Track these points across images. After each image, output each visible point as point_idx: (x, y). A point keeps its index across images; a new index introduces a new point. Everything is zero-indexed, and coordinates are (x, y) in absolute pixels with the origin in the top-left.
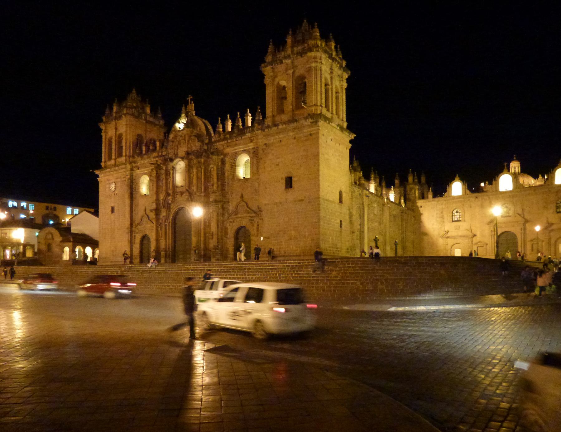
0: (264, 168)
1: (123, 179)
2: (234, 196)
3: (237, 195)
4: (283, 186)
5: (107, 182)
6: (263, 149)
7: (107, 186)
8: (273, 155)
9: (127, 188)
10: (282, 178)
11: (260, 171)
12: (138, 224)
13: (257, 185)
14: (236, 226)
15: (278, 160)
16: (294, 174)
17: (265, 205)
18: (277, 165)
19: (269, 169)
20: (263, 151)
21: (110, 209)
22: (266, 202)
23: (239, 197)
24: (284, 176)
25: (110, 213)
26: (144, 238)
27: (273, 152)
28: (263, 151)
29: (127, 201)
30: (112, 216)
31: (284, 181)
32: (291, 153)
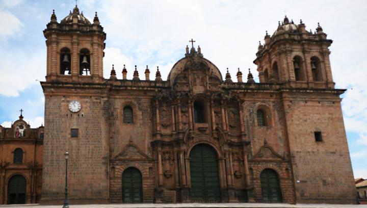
0: (292, 120)
1: (95, 101)
2: (255, 139)
3: (259, 140)
4: (312, 138)
5: (63, 99)
6: (288, 105)
7: (62, 103)
8: (299, 111)
9: (102, 112)
10: (311, 132)
11: (288, 123)
12: (120, 155)
13: (280, 134)
14: (262, 167)
15: (305, 117)
16: (322, 131)
17: (297, 152)
18: (305, 121)
19: (297, 122)
20: (290, 107)
21: (69, 132)
22: (298, 150)
23: (262, 142)
24: (314, 130)
25: (70, 136)
26: (131, 171)
27: (299, 109)
28: (290, 107)
29: (103, 126)
30: (74, 142)
31: (313, 135)
32: (317, 114)
